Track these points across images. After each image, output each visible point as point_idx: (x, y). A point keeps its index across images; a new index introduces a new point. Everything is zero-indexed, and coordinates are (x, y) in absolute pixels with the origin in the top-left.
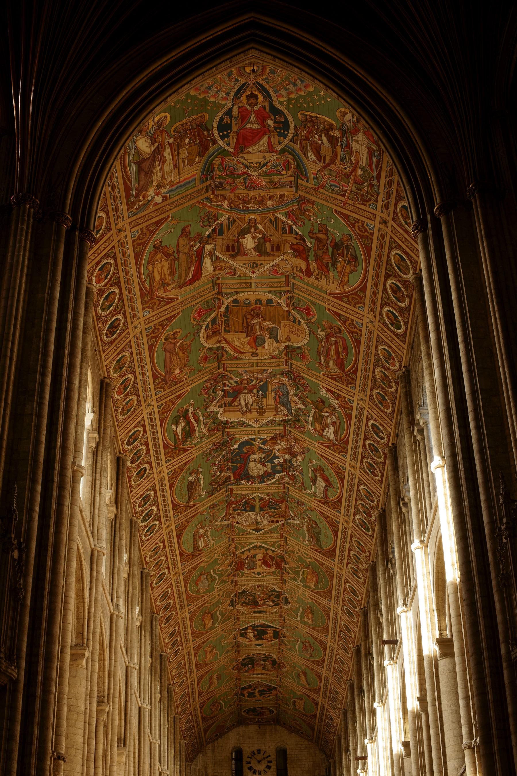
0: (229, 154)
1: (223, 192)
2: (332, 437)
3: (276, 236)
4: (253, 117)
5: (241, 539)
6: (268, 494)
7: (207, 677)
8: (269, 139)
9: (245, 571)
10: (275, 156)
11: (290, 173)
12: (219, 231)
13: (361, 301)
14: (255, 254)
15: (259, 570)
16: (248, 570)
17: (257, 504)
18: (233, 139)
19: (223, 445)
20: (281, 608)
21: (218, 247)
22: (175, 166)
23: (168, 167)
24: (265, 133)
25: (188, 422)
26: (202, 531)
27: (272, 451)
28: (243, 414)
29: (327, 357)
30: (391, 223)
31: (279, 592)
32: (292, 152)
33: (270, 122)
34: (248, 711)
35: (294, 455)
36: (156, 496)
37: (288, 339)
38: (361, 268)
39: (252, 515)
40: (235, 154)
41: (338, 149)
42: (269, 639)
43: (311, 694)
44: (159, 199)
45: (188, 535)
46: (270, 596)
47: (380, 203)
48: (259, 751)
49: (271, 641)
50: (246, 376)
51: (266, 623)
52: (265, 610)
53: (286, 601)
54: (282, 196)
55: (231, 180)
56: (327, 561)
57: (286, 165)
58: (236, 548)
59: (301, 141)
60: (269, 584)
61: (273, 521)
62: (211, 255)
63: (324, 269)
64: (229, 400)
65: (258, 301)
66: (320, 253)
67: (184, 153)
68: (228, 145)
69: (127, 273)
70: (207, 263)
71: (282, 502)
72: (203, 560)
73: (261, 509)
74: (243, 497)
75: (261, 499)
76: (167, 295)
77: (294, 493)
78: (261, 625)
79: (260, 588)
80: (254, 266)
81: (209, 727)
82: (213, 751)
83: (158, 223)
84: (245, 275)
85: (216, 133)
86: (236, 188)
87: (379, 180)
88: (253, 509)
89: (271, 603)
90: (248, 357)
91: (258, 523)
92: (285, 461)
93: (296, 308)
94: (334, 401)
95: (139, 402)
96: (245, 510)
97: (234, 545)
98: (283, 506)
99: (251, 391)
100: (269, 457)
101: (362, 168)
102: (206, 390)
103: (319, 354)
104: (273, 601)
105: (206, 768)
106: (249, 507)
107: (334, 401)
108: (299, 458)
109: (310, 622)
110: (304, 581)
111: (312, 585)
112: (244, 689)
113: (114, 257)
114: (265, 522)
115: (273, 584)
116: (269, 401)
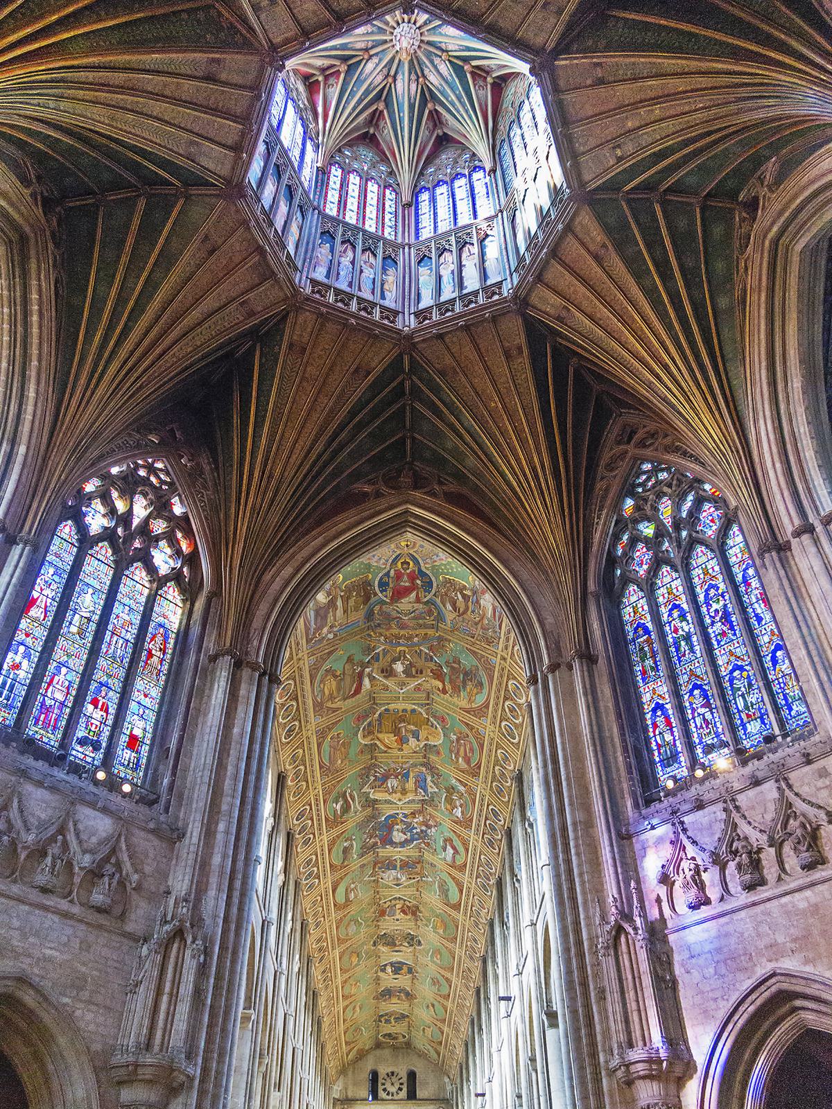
0: (386, 603)
1: (381, 631)
2: (459, 815)
3: (420, 663)
4: (405, 578)
5: (383, 891)
6: (408, 857)
7: (350, 1007)
8: (417, 593)
9: (387, 917)
10: (421, 606)
11: (432, 618)
12: (376, 658)
13: (485, 715)
14: (403, 676)
15: (398, 917)
17: (398, 864)
18: (389, 593)
19: (373, 817)
21: (375, 670)
22: (344, 612)
23: (339, 612)
24: (414, 589)
25: (346, 801)
26: (352, 886)
29: (457, 754)
30: (509, 659)
32: (434, 604)
33: (419, 582)
34: (384, 1036)
35: (429, 827)
36: (317, 859)
37: (427, 739)
38: (485, 691)
40: (391, 604)
41: (470, 603)
43: (438, 1023)
44: (331, 636)
45: (341, 890)
47: (501, 646)
48: (393, 1073)
50: (393, 766)
53: (419, 943)
54: (426, 634)
55: (387, 622)
56: (453, 913)
57: (430, 613)
58: (380, 899)
59: (442, 596)
62: (369, 675)
63: (457, 690)
64: (378, 783)
65: (403, 710)
66: (453, 677)
67: (352, 602)
68: (386, 596)
69: (303, 690)
70: (366, 681)
72: (353, 909)
73: (401, 868)
74: (388, 858)
75: (401, 861)
76: (334, 706)
77: (428, 856)
80: (402, 685)
81: (350, 1051)
82: (353, 1072)
83: (330, 653)
84: (395, 690)
85: (377, 588)
86: (391, 628)
87: (500, 628)
90: (396, 752)
91: (398, 879)
92: (422, 831)
93: (434, 717)
94: (462, 788)
95: (308, 786)
96: (389, 869)
98: (419, 866)
99: (396, 777)
100: (409, 828)
101: (488, 619)
102: (361, 776)
103: (451, 751)
105: (346, 1089)
106: (390, 865)
108: (433, 830)
109: (438, 962)
110: (435, 928)
111: (441, 931)
112: (382, 1016)
113: (294, 680)
114: (404, 879)
116: (410, 784)
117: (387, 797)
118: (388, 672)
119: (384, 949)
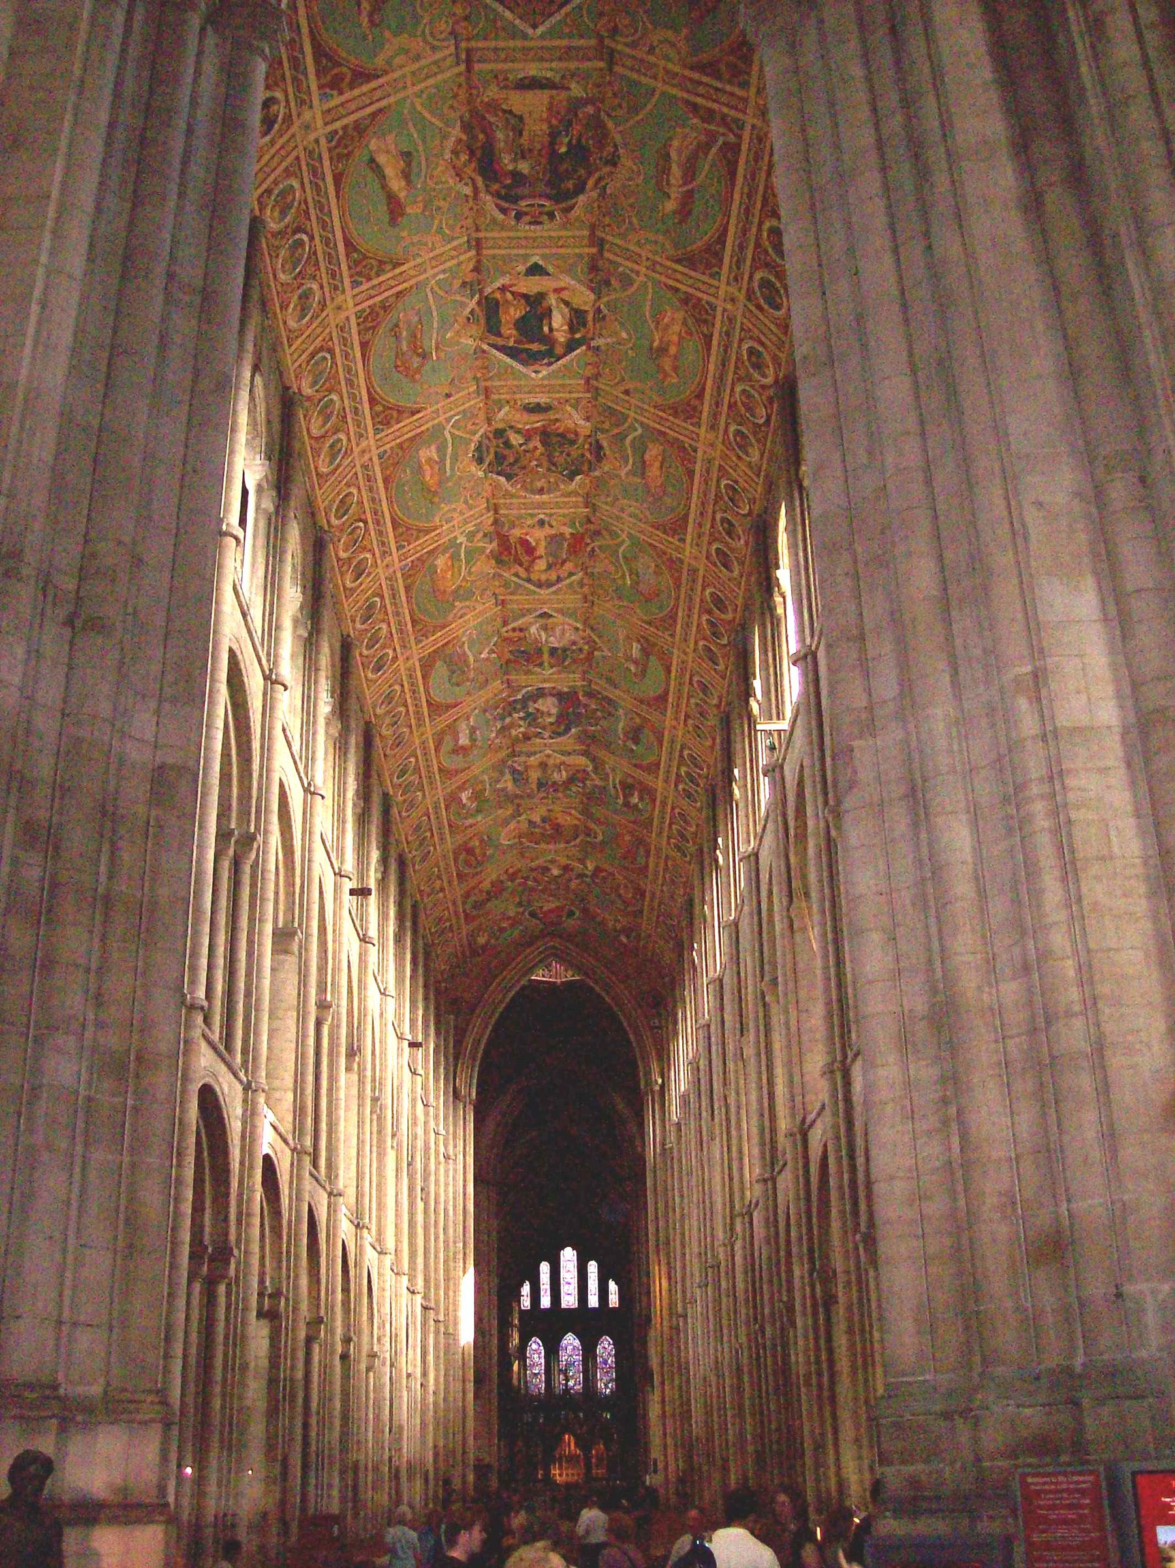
5: (572, 600)
6: (528, 672)
9: (567, 531)
12: (580, 876)
16: (562, 534)
20: (489, 421)
27: (530, 725)
28: (564, 763)
31: (499, 474)
38: (468, 906)
39: (554, 642)
42: (509, 296)
46: (517, 461)
49: (503, 289)
51: (520, 367)
52: (526, 417)
58: (581, 584)
60: (520, 497)
61: (521, 630)
71: (508, 662)
73: (539, 652)
75: (541, 665)
78: (528, 358)
79: (539, 484)
80: (552, 861)
88: (553, 651)
89: (516, 439)
90: (556, 808)
91: (545, 628)
94: (470, 821)
96: (565, 650)
97: (586, 589)
98: (508, 656)
99: (554, 783)
100: (532, 718)
104: (507, 444)
107: (470, 821)
114: (533, 630)
115: (512, 496)
116: (534, 775)
117: (569, 760)
118: (566, 868)
119: (575, 420)
